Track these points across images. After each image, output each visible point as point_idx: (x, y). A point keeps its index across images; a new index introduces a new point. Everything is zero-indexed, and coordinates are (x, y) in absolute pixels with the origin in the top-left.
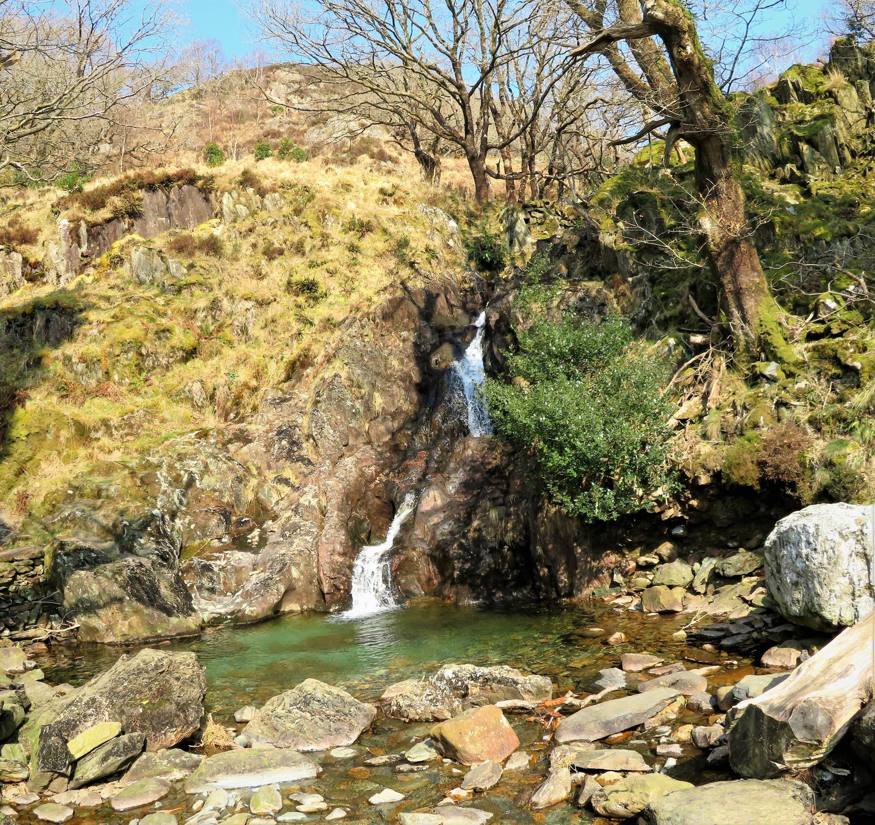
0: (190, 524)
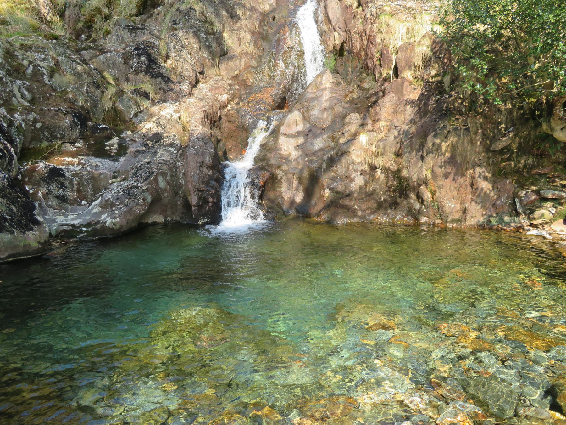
0: (35, 121)
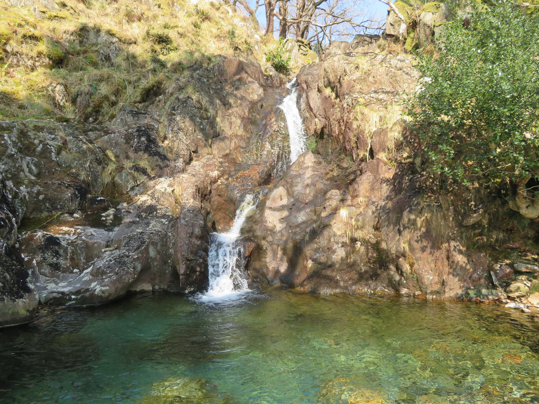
0: (39, 193)
